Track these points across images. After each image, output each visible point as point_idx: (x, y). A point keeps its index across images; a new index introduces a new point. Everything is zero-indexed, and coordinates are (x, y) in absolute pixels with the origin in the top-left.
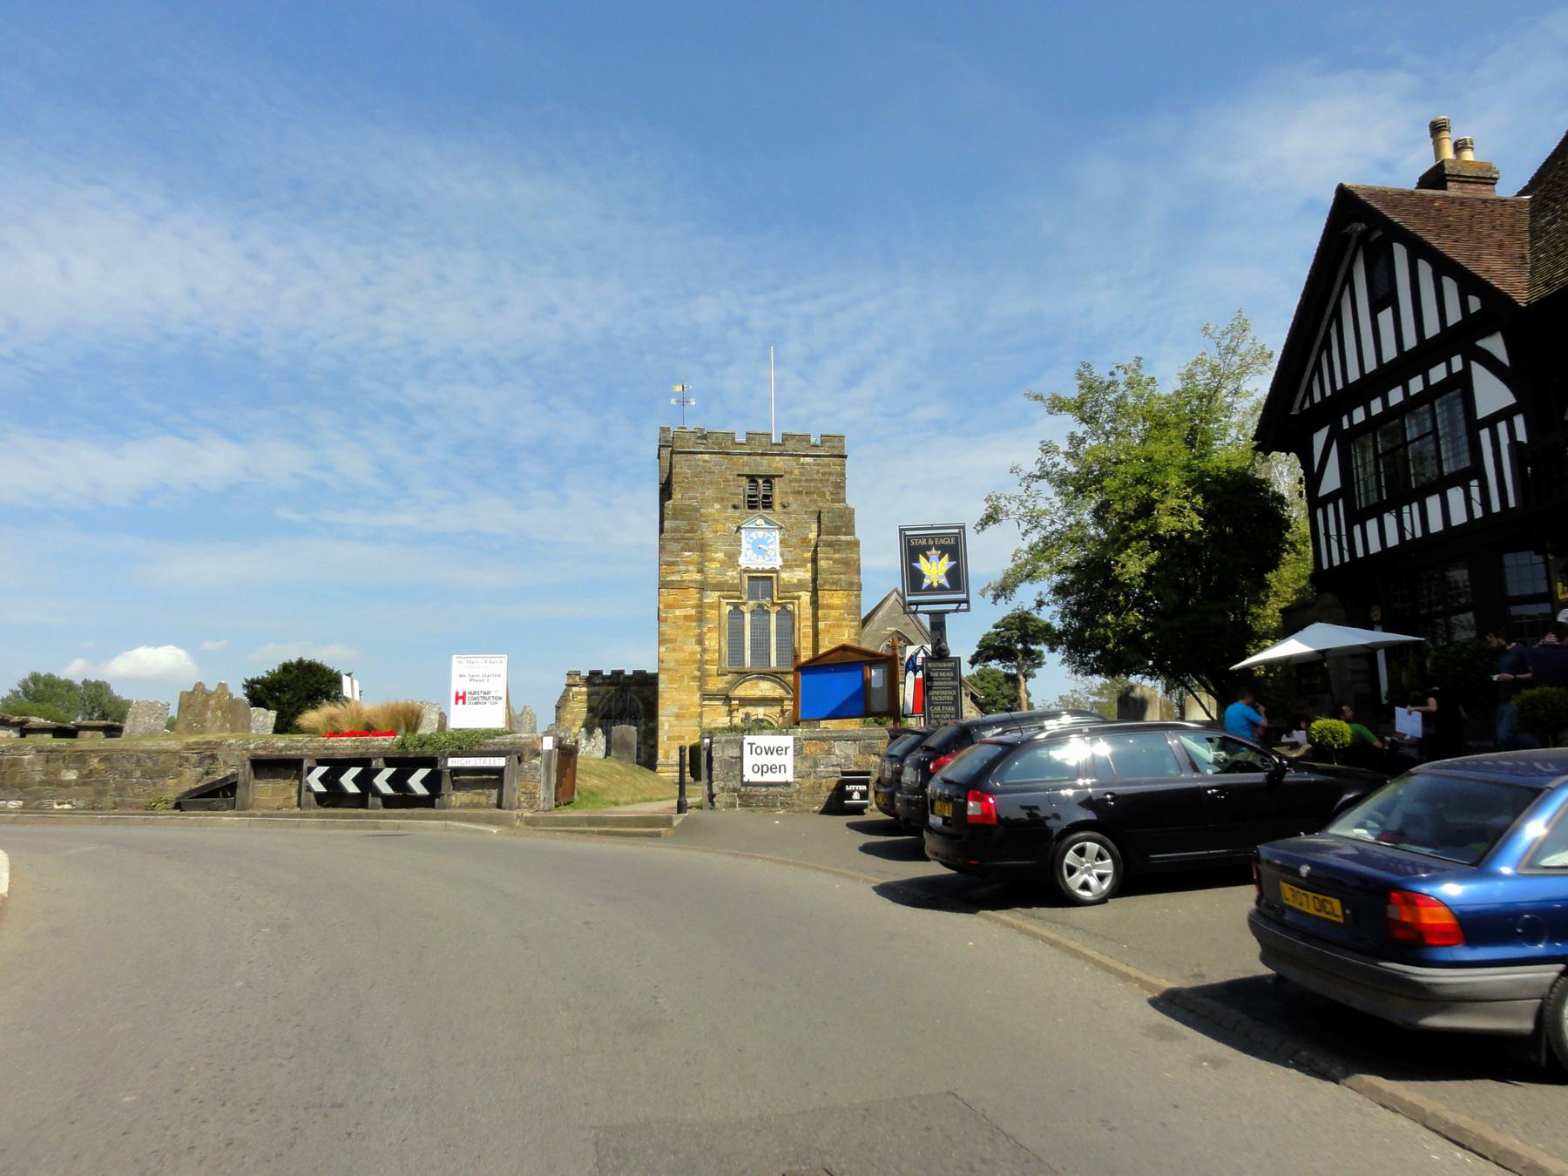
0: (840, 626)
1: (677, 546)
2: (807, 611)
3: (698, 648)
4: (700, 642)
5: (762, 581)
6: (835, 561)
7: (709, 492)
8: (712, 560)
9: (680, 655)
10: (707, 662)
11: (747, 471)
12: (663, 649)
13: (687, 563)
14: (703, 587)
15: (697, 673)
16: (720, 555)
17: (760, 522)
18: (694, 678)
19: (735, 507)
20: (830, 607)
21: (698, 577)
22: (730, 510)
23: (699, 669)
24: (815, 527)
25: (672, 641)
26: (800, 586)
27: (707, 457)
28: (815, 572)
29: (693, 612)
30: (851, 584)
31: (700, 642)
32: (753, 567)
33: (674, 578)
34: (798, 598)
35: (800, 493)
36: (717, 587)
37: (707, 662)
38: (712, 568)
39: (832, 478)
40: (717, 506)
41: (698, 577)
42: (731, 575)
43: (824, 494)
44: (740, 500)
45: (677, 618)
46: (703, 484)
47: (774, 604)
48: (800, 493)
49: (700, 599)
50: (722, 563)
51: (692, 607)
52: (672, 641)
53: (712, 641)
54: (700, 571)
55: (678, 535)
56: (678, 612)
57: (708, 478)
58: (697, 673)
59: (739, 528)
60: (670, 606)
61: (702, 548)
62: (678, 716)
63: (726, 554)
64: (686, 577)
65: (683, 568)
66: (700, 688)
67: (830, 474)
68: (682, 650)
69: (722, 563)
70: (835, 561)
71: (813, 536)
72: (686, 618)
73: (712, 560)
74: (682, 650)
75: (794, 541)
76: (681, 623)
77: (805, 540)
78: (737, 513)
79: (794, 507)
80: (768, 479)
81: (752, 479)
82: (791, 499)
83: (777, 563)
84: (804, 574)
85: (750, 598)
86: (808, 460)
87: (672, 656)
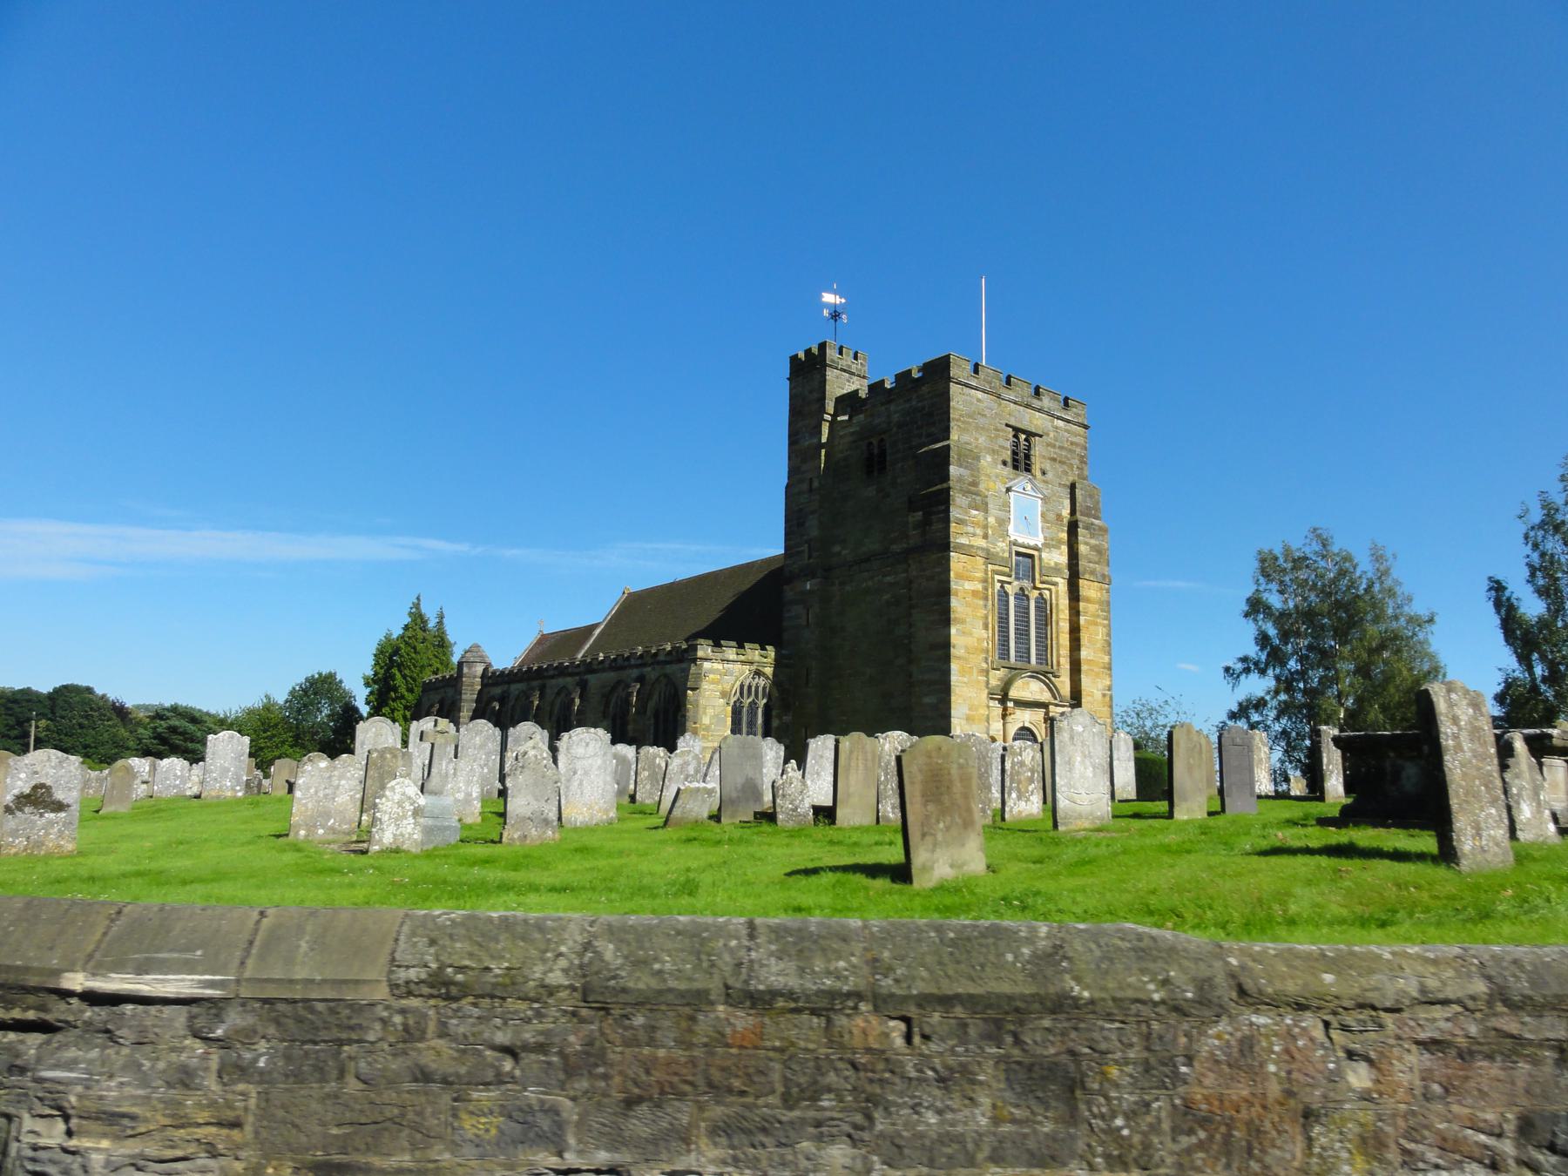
0: (1096, 624)
2: (1064, 602)
5: (1027, 559)
6: (1093, 548)
11: (1012, 423)
17: (1029, 487)
19: (1005, 463)
20: (1088, 600)
22: (1000, 466)
24: (1067, 503)
25: (963, 622)
26: (1056, 570)
27: (980, 395)
28: (1073, 556)
30: (1103, 576)
32: (1020, 541)
33: (963, 540)
34: (1055, 584)
35: (1054, 460)
40: (989, 458)
41: (982, 543)
42: (1001, 547)
44: (1007, 455)
45: (966, 592)
46: (977, 428)
47: (1035, 588)
48: (1054, 460)
57: (981, 421)
59: (1008, 490)
61: (984, 508)
65: (970, 529)
67: (1077, 445)
68: (971, 634)
70: (1093, 548)
71: (1066, 512)
72: (975, 593)
75: (1052, 516)
77: (1059, 517)
79: (1050, 475)
80: (1030, 434)
81: (1017, 431)
82: (1047, 466)
83: (1038, 540)
84: (1060, 557)
85: (1017, 578)
86: (1061, 423)
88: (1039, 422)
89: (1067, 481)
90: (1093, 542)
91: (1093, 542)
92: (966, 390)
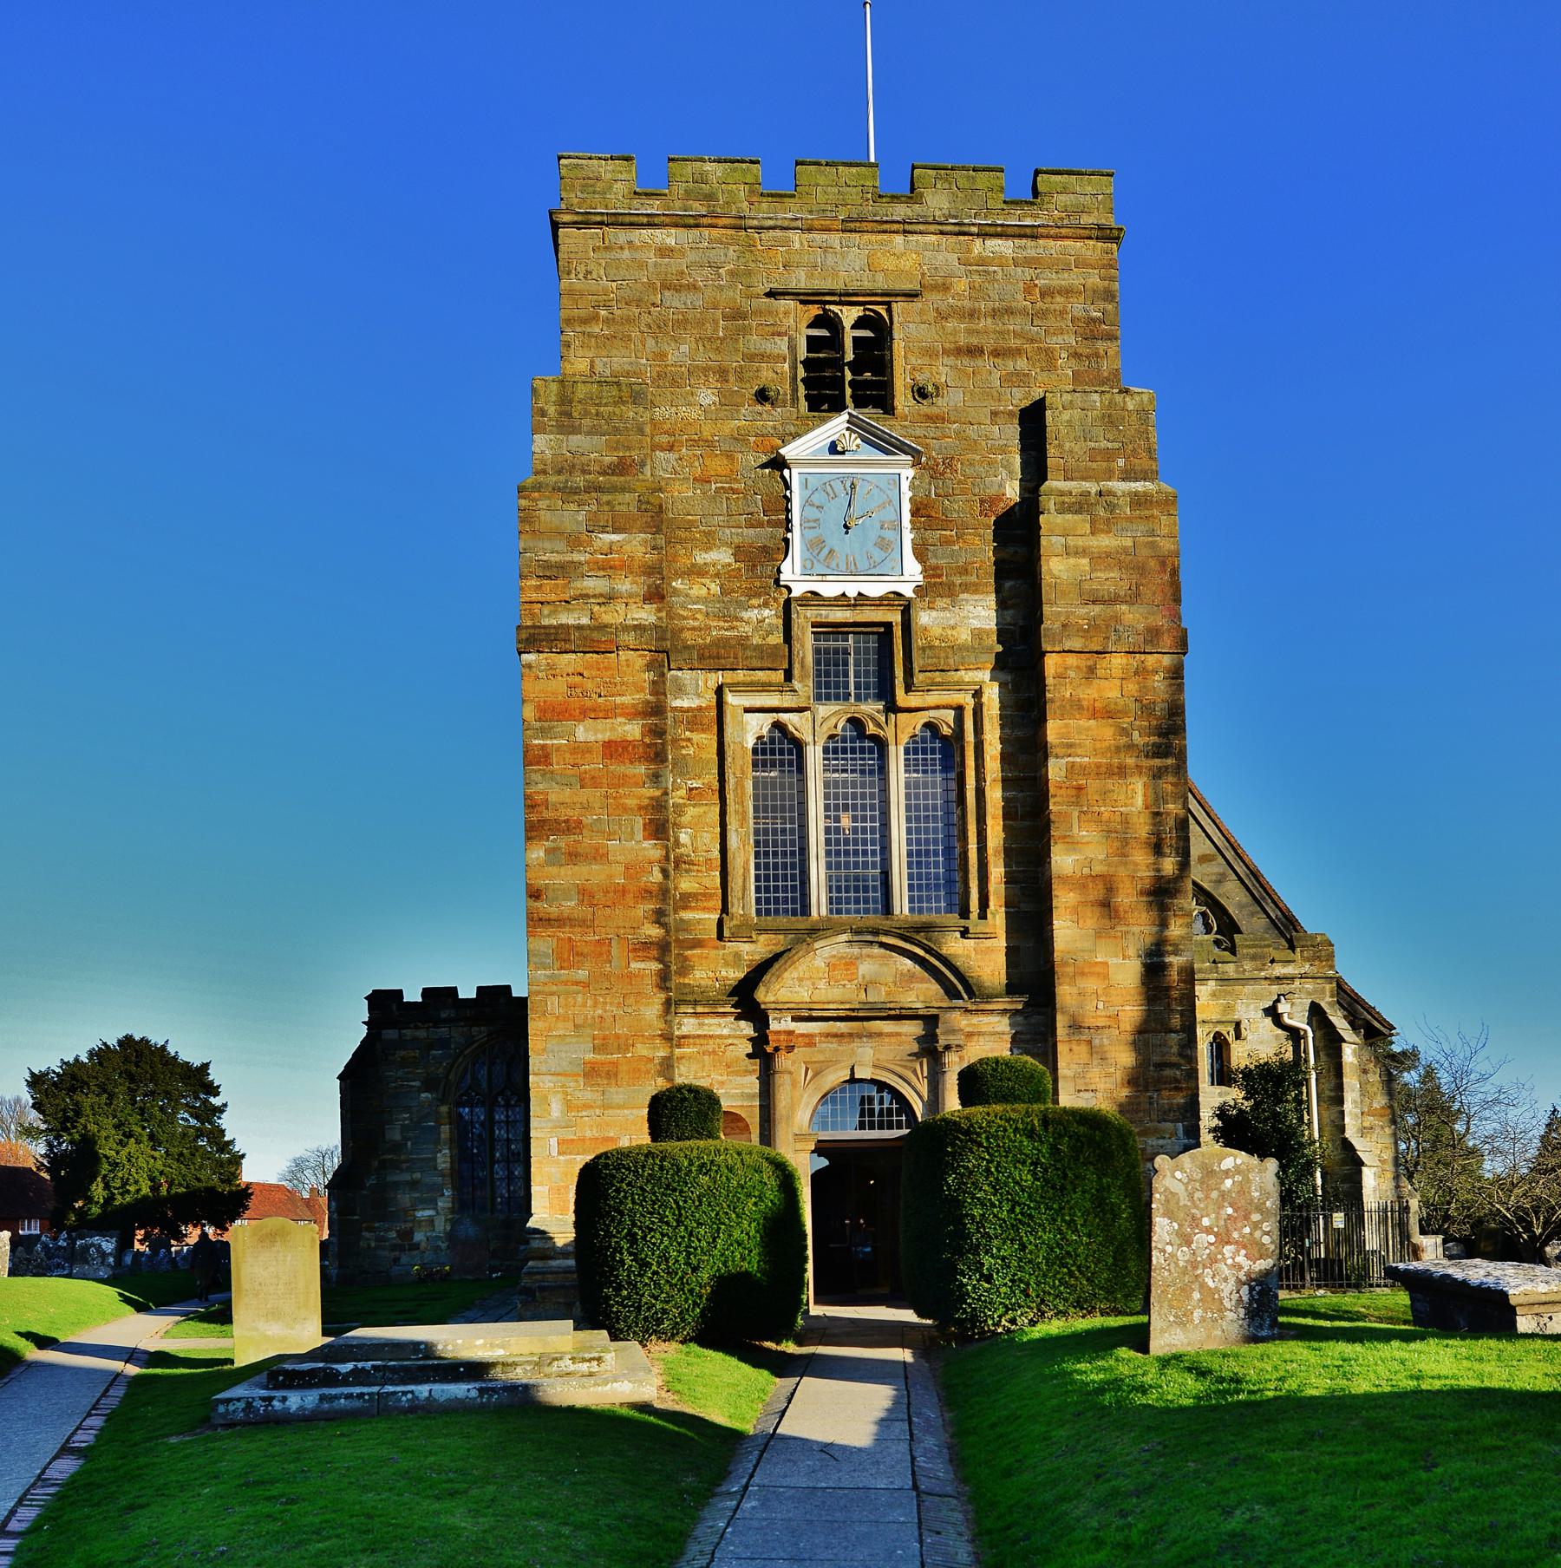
1: (573, 517)
3: (651, 850)
4: (659, 828)
6: (1100, 559)
7: (681, 353)
8: (697, 572)
9: (593, 874)
10: (686, 900)
11: (800, 280)
12: (537, 853)
13: (606, 568)
14: (666, 650)
15: (654, 932)
16: (722, 556)
18: (643, 948)
21: (646, 615)
23: (659, 917)
27: (669, 237)
29: (633, 730)
31: (659, 828)
32: (829, 590)
35: (974, 352)
36: (713, 657)
37: (686, 900)
38: (695, 597)
39: (1077, 307)
41: (646, 615)
43: (1049, 355)
44: (782, 374)
45: (580, 749)
48: (974, 352)
49: (658, 688)
50: (725, 576)
51: (634, 714)
52: (571, 827)
53: (696, 834)
54: (655, 596)
55: (579, 480)
56: (584, 732)
58: (654, 932)
60: (553, 713)
62: (591, 1073)
63: (738, 552)
64: (611, 616)
66: (663, 979)
67: (1067, 292)
69: (725, 576)
72: (613, 749)
73: (697, 572)
74: (599, 856)
76: (594, 765)
78: (771, 418)
79: (951, 400)
87: (564, 876)
88: (908, 263)
89: (1020, 399)
90: (1105, 542)
91: (1105, 542)
92: (621, 236)
